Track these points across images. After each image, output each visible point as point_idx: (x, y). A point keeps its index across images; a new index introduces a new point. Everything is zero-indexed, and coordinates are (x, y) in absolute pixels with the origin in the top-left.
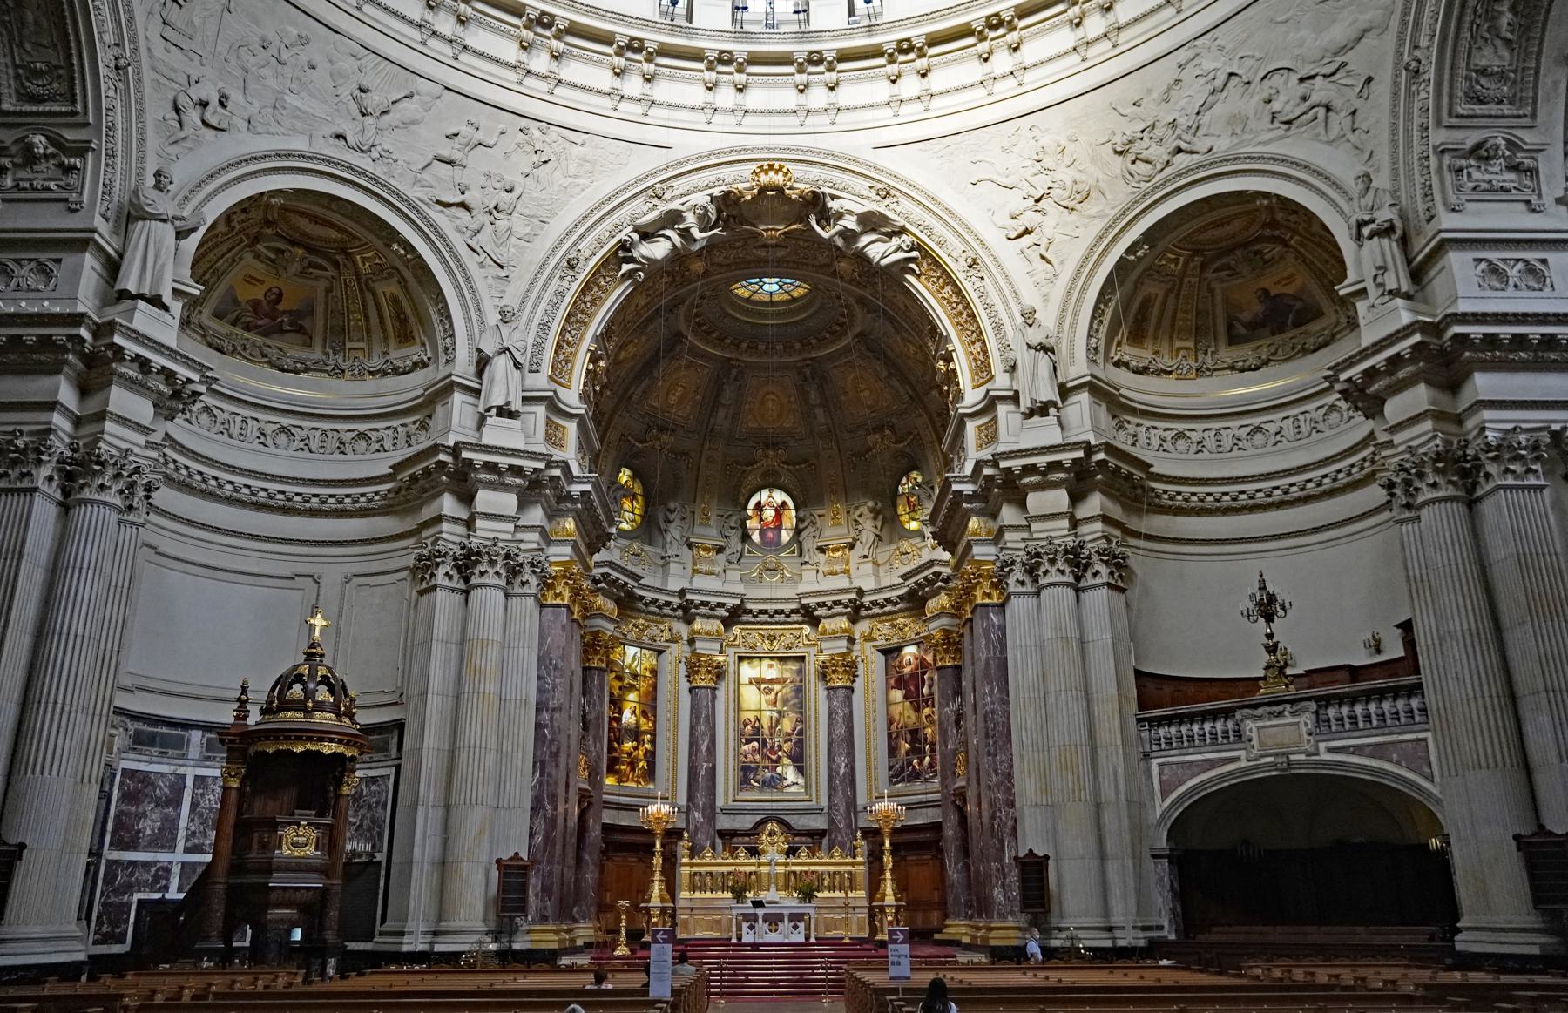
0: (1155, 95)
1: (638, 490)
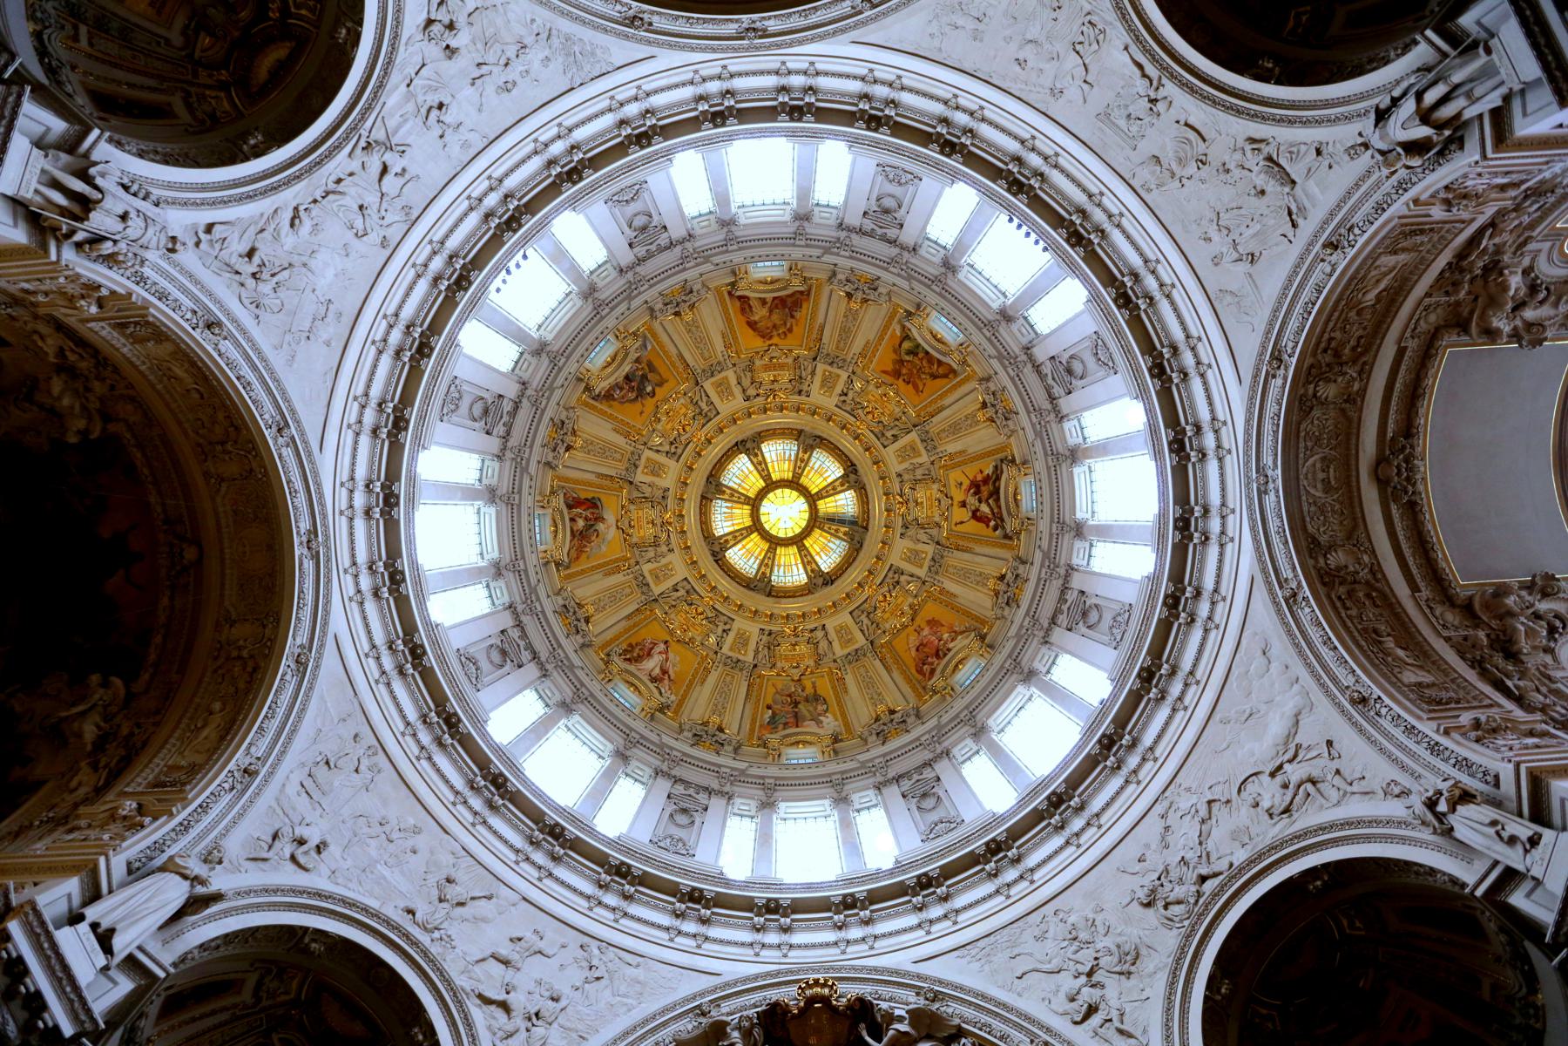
0: (1153, 846)
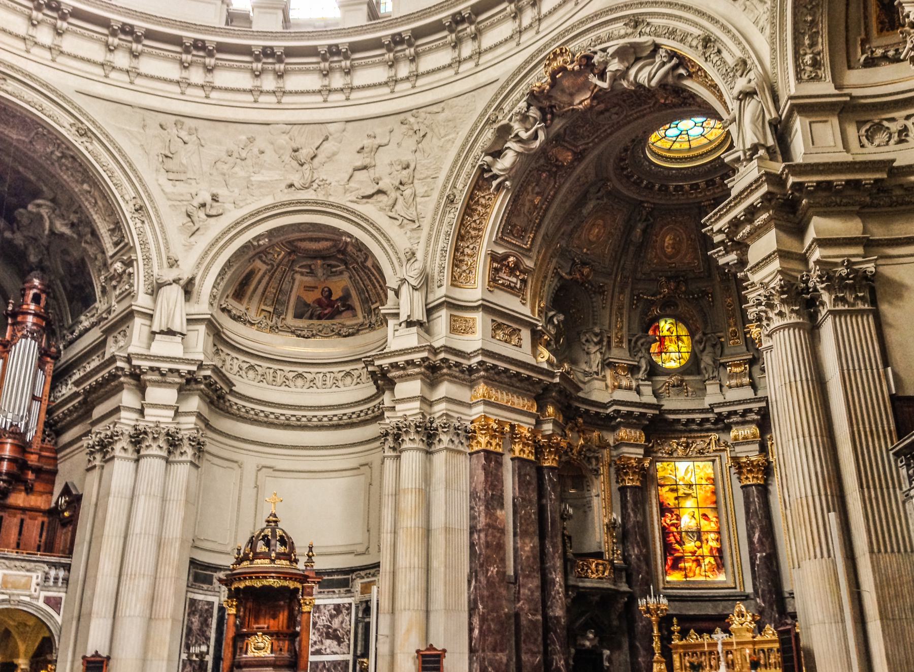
1: (683, 331)
